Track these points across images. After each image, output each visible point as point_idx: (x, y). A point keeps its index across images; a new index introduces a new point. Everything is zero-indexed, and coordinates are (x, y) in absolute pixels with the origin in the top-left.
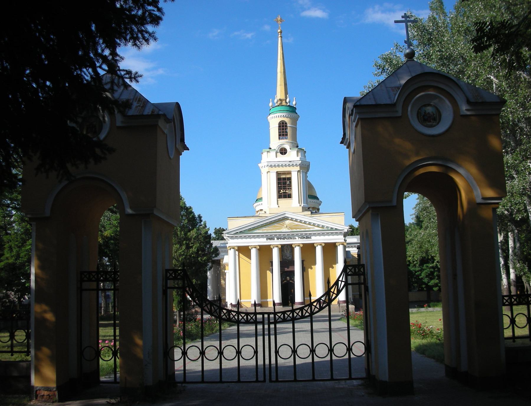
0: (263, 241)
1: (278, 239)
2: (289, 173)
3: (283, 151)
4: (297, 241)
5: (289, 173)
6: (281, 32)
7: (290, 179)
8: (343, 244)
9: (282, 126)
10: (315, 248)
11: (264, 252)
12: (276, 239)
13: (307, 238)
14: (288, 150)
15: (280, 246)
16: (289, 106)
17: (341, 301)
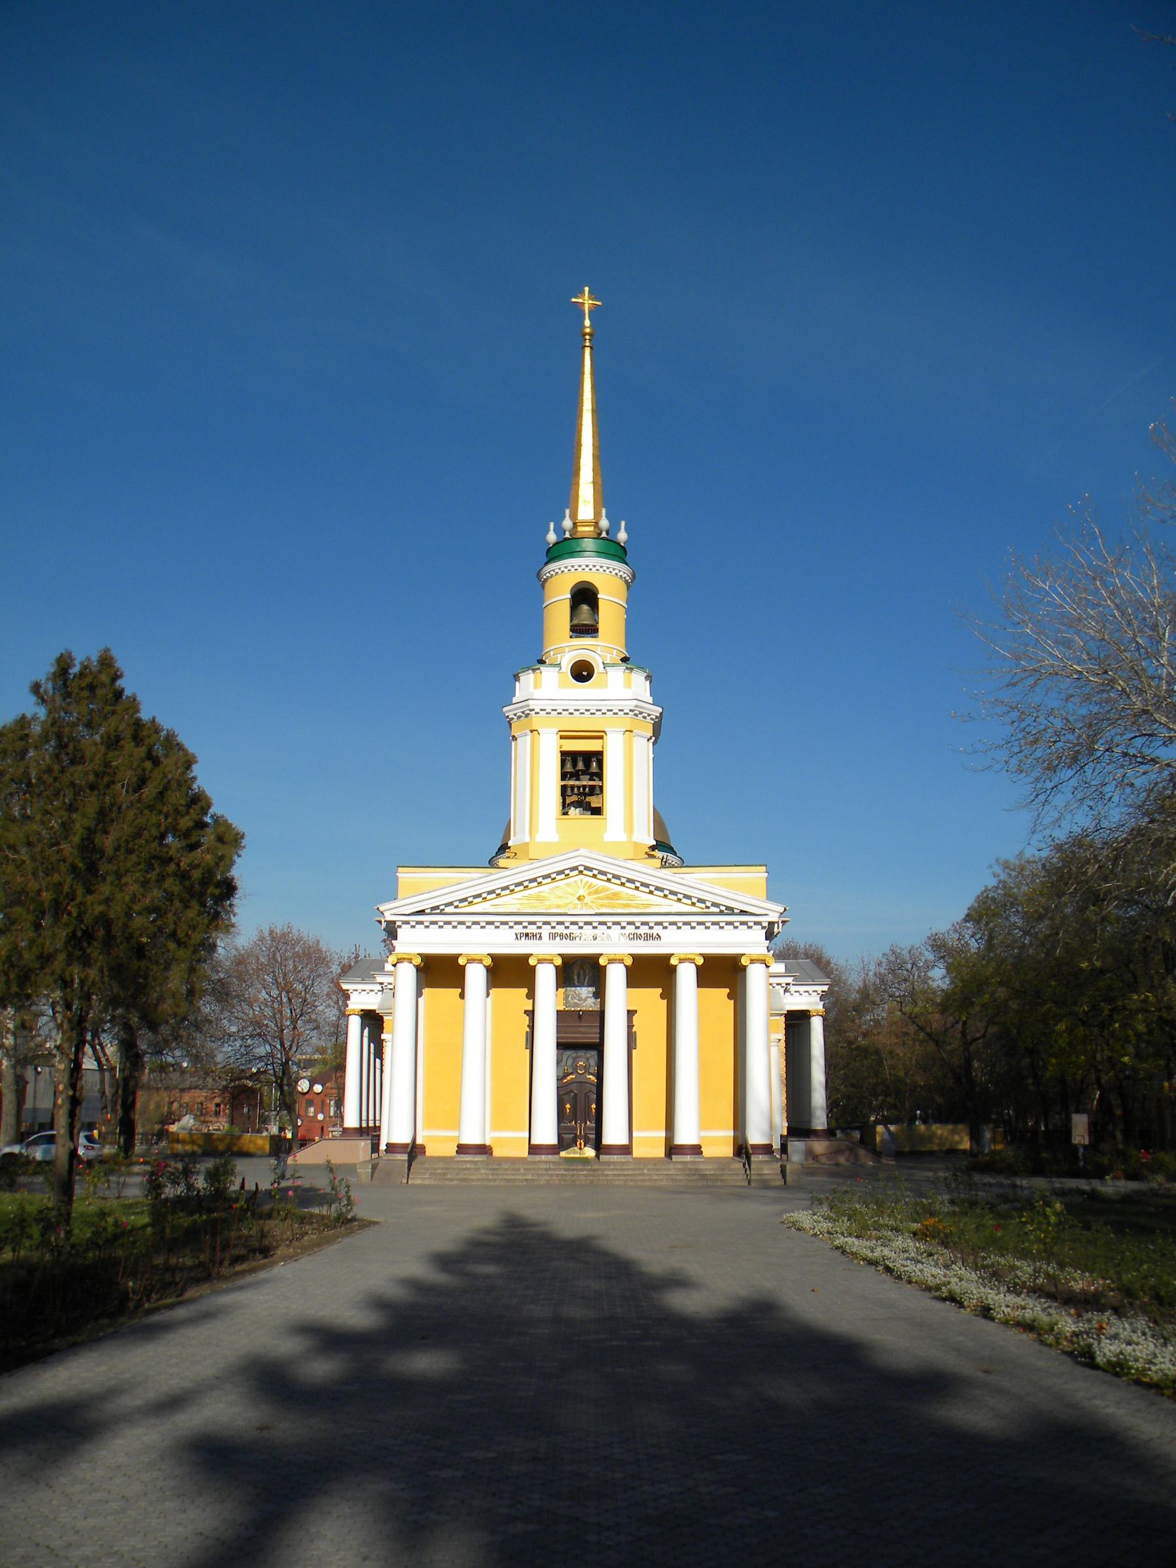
0: (506, 943)
1: (553, 936)
2: (599, 736)
3: (582, 672)
4: (614, 946)
5: (599, 736)
6: (590, 334)
7: (598, 756)
8: (763, 962)
9: (584, 596)
10: (673, 969)
11: (510, 972)
12: (545, 936)
13: (648, 937)
14: (598, 668)
15: (559, 962)
16: (603, 539)
17: (754, 1147)
